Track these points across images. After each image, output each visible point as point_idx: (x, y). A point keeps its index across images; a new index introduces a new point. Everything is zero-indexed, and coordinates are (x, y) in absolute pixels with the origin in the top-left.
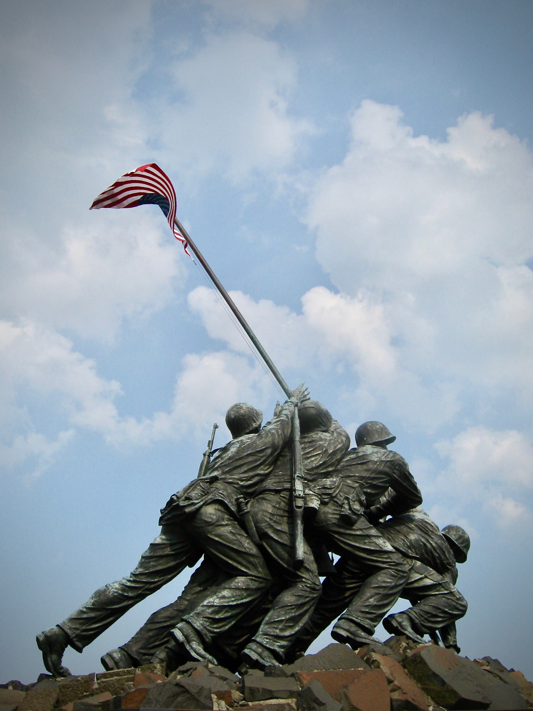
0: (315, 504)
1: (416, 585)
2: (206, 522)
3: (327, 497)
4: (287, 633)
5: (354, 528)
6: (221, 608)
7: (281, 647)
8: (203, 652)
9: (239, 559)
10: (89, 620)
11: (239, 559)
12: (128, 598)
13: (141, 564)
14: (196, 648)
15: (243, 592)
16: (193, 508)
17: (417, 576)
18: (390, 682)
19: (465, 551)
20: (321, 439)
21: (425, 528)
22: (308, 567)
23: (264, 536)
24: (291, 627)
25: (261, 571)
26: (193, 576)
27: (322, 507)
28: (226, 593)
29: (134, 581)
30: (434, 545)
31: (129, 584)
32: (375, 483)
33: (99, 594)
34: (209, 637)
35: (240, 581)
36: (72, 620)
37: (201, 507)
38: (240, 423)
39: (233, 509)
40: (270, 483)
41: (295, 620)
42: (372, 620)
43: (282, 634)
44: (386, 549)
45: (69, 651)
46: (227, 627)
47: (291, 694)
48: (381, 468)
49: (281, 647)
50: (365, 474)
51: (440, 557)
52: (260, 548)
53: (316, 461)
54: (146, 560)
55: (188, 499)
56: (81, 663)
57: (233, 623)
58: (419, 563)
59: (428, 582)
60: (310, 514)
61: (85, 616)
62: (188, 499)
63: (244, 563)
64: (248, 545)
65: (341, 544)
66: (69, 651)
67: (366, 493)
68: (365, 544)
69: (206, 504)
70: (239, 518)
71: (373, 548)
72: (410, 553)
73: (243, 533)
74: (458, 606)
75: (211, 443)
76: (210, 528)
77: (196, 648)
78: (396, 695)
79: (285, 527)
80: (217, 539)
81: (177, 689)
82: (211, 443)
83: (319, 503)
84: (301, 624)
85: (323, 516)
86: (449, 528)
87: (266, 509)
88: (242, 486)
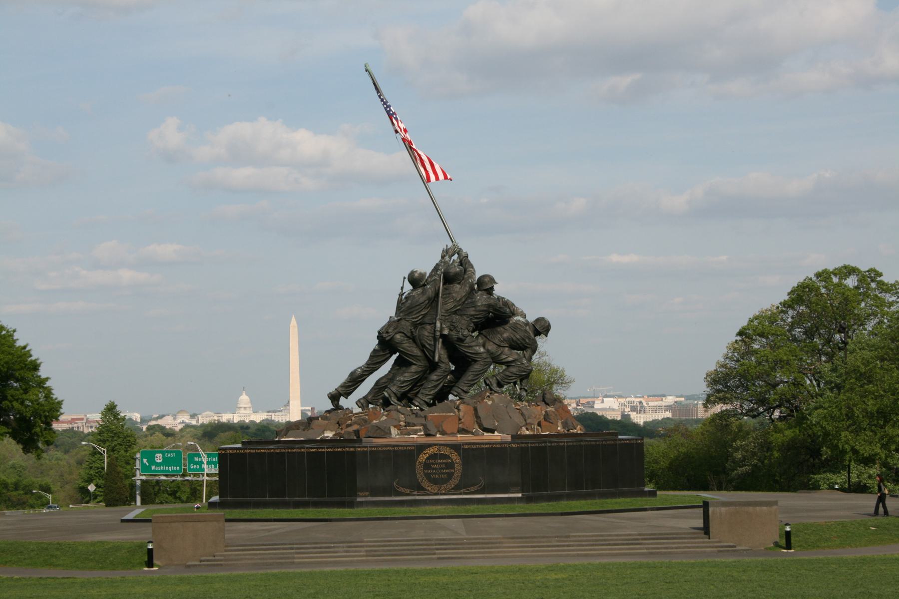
0: (446, 332)
3: (452, 327)
6: (404, 382)
14: (394, 400)
18: (460, 419)
23: (424, 346)
25: (424, 363)
26: (396, 360)
28: (406, 375)
33: (352, 374)
34: (399, 395)
35: (413, 368)
36: (341, 386)
38: (415, 280)
39: (409, 334)
40: (427, 320)
41: (436, 386)
45: (342, 398)
47: (422, 425)
48: (482, 308)
50: (473, 313)
52: (423, 351)
53: (450, 305)
54: (371, 357)
55: (387, 332)
56: (349, 403)
59: (510, 359)
62: (387, 332)
64: (417, 352)
66: (342, 398)
70: (413, 339)
72: (502, 344)
73: (414, 345)
75: (402, 288)
77: (394, 400)
78: (461, 426)
79: (432, 343)
82: (402, 288)
84: (439, 388)
86: (538, 320)
87: (426, 332)
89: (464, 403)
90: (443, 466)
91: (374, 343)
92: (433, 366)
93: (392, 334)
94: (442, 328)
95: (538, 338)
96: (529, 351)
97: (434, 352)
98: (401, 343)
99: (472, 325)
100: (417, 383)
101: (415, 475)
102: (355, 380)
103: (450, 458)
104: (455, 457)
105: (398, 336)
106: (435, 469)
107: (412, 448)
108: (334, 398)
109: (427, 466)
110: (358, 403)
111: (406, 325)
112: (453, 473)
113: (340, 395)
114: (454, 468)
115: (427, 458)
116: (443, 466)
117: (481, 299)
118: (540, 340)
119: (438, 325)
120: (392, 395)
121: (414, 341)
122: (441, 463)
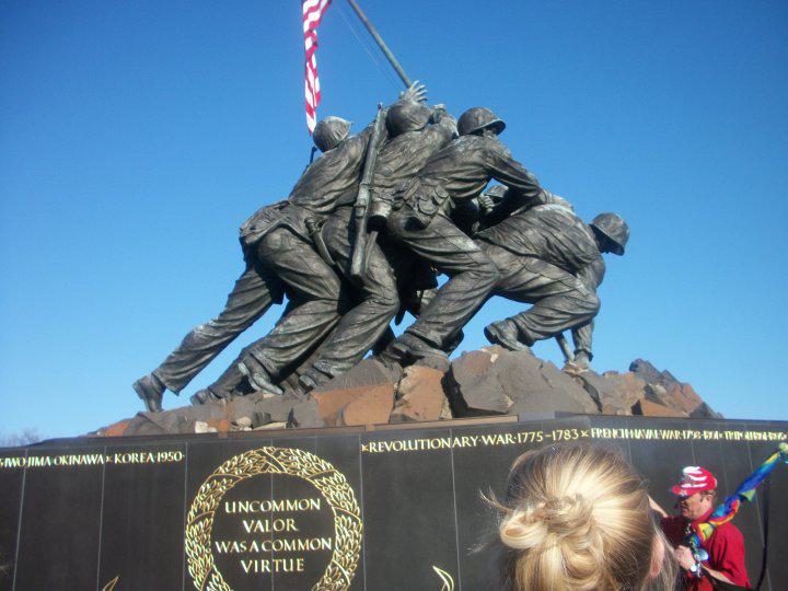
0: (383, 211)
1: (530, 286)
2: (273, 250)
4: (347, 355)
5: (427, 230)
7: (343, 369)
8: (262, 381)
9: (310, 284)
10: (179, 364)
11: (310, 284)
12: (215, 338)
13: (228, 305)
14: (260, 379)
15: (311, 317)
16: (255, 238)
17: (531, 276)
18: (398, 396)
19: (619, 240)
20: (407, 140)
21: (550, 222)
22: (378, 281)
23: (336, 255)
24: (353, 347)
27: (395, 213)
29: (219, 321)
30: (560, 237)
31: (214, 324)
32: (459, 176)
34: (273, 368)
37: (265, 236)
39: (301, 230)
42: (439, 330)
43: (341, 356)
44: (465, 249)
46: (296, 356)
49: (337, 369)
51: (570, 252)
52: (335, 269)
57: (304, 350)
58: (535, 260)
59: (544, 280)
60: (376, 223)
61: (173, 360)
63: (314, 286)
64: (316, 266)
65: (420, 253)
66: (168, 395)
67: (450, 191)
68: (440, 246)
69: (273, 230)
71: (448, 250)
72: (523, 250)
73: (314, 255)
74: (584, 304)
76: (277, 255)
77: (260, 379)
78: (398, 411)
80: (283, 265)
81: (141, 420)
83: (390, 208)
85: (394, 224)
86: (601, 217)
88: (315, 207)
89: (424, 365)
90: (290, 525)
91: (238, 266)
92: (354, 292)
93: (263, 227)
94: (372, 204)
95: (604, 255)
96: (589, 272)
97: (350, 261)
98: (282, 251)
99: (445, 194)
100: (321, 340)
101: (180, 559)
102: (192, 355)
103: (316, 494)
104: (338, 491)
105: (276, 236)
106: (259, 536)
107: (175, 457)
108: (150, 392)
109: (226, 527)
110: (196, 398)
111: (302, 219)
112: (326, 555)
113: (163, 388)
114: (329, 532)
115: (232, 495)
116: (290, 525)
117: (469, 150)
118: (609, 258)
119: (363, 195)
120: (258, 369)
121: (316, 248)
122: (285, 515)
